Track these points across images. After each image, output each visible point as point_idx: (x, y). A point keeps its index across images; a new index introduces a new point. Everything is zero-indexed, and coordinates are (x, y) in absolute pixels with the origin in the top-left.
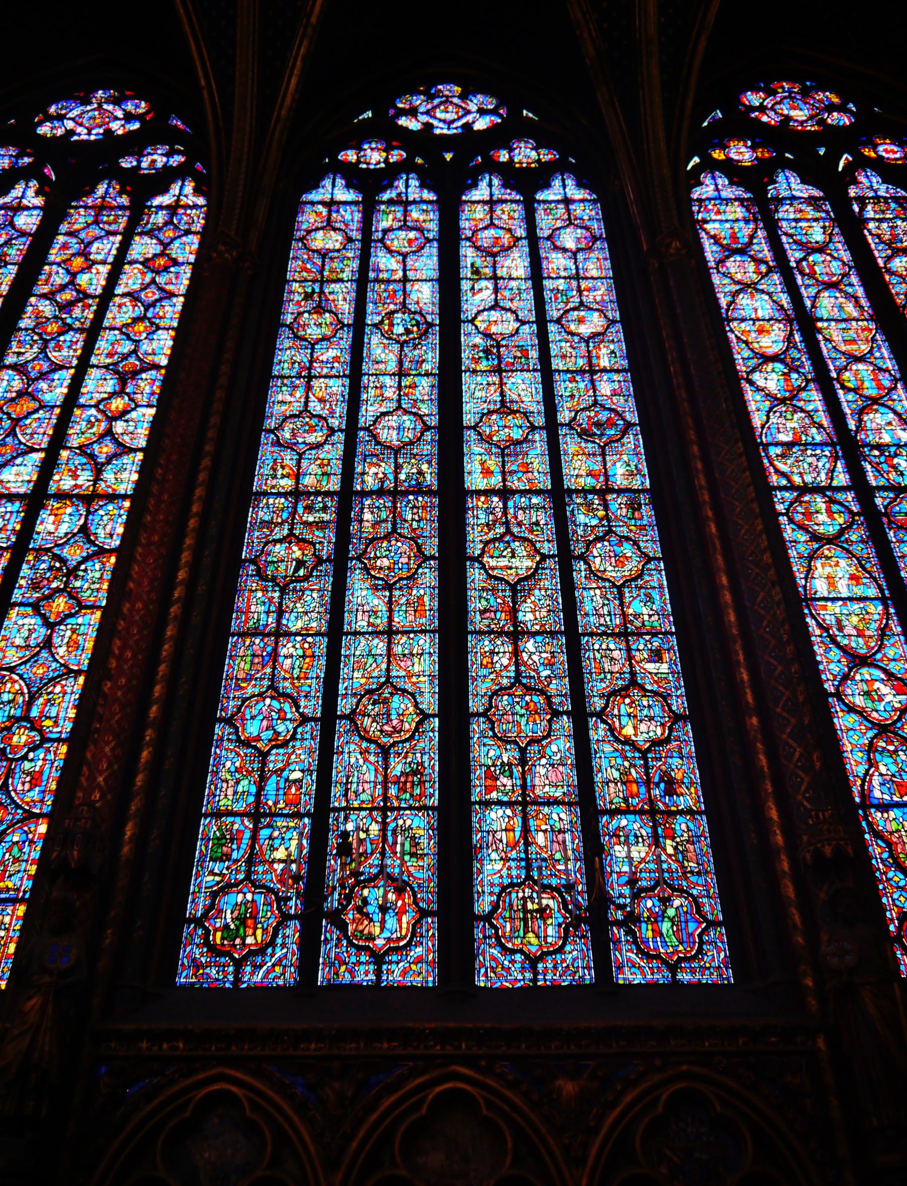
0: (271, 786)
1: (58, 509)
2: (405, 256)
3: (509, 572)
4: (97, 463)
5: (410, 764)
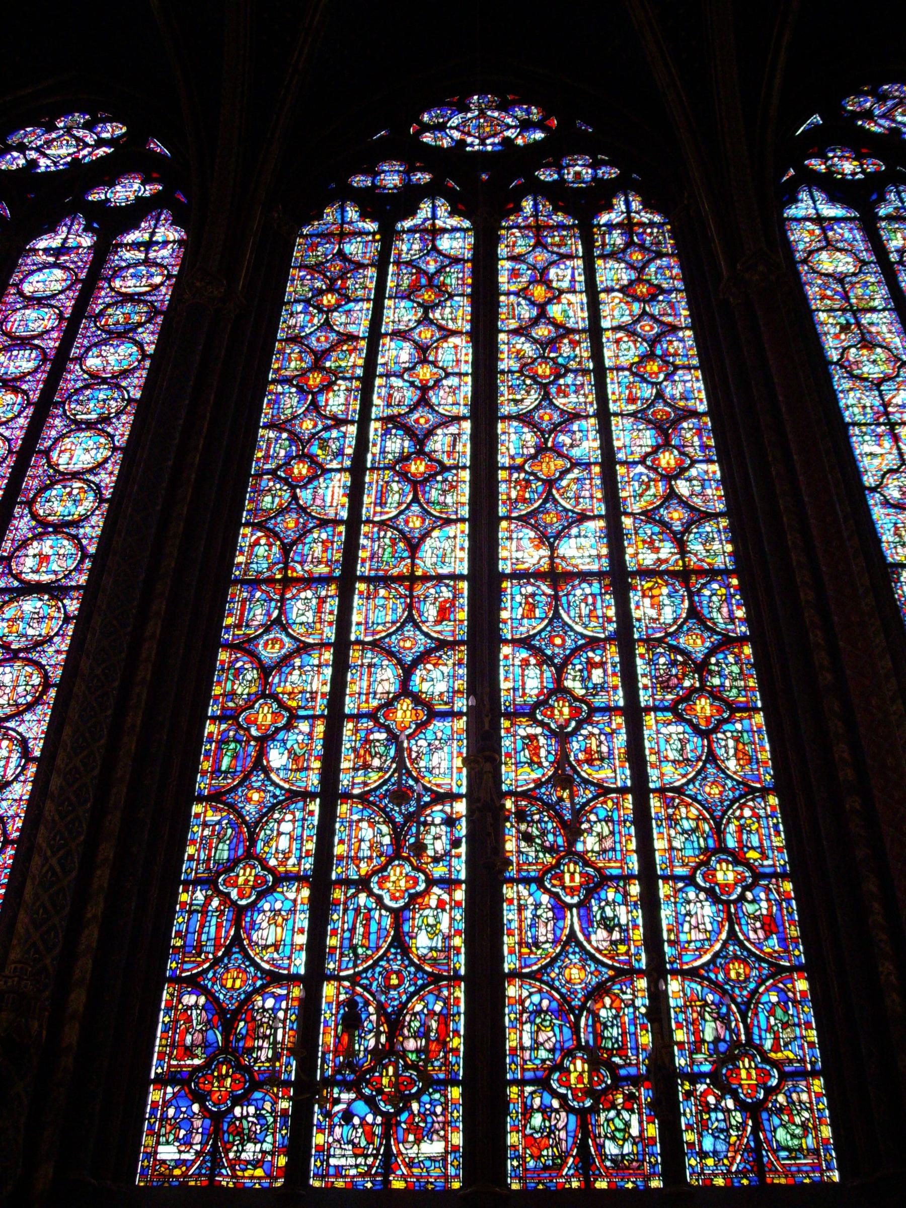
1: (650, 589)
4: (674, 533)
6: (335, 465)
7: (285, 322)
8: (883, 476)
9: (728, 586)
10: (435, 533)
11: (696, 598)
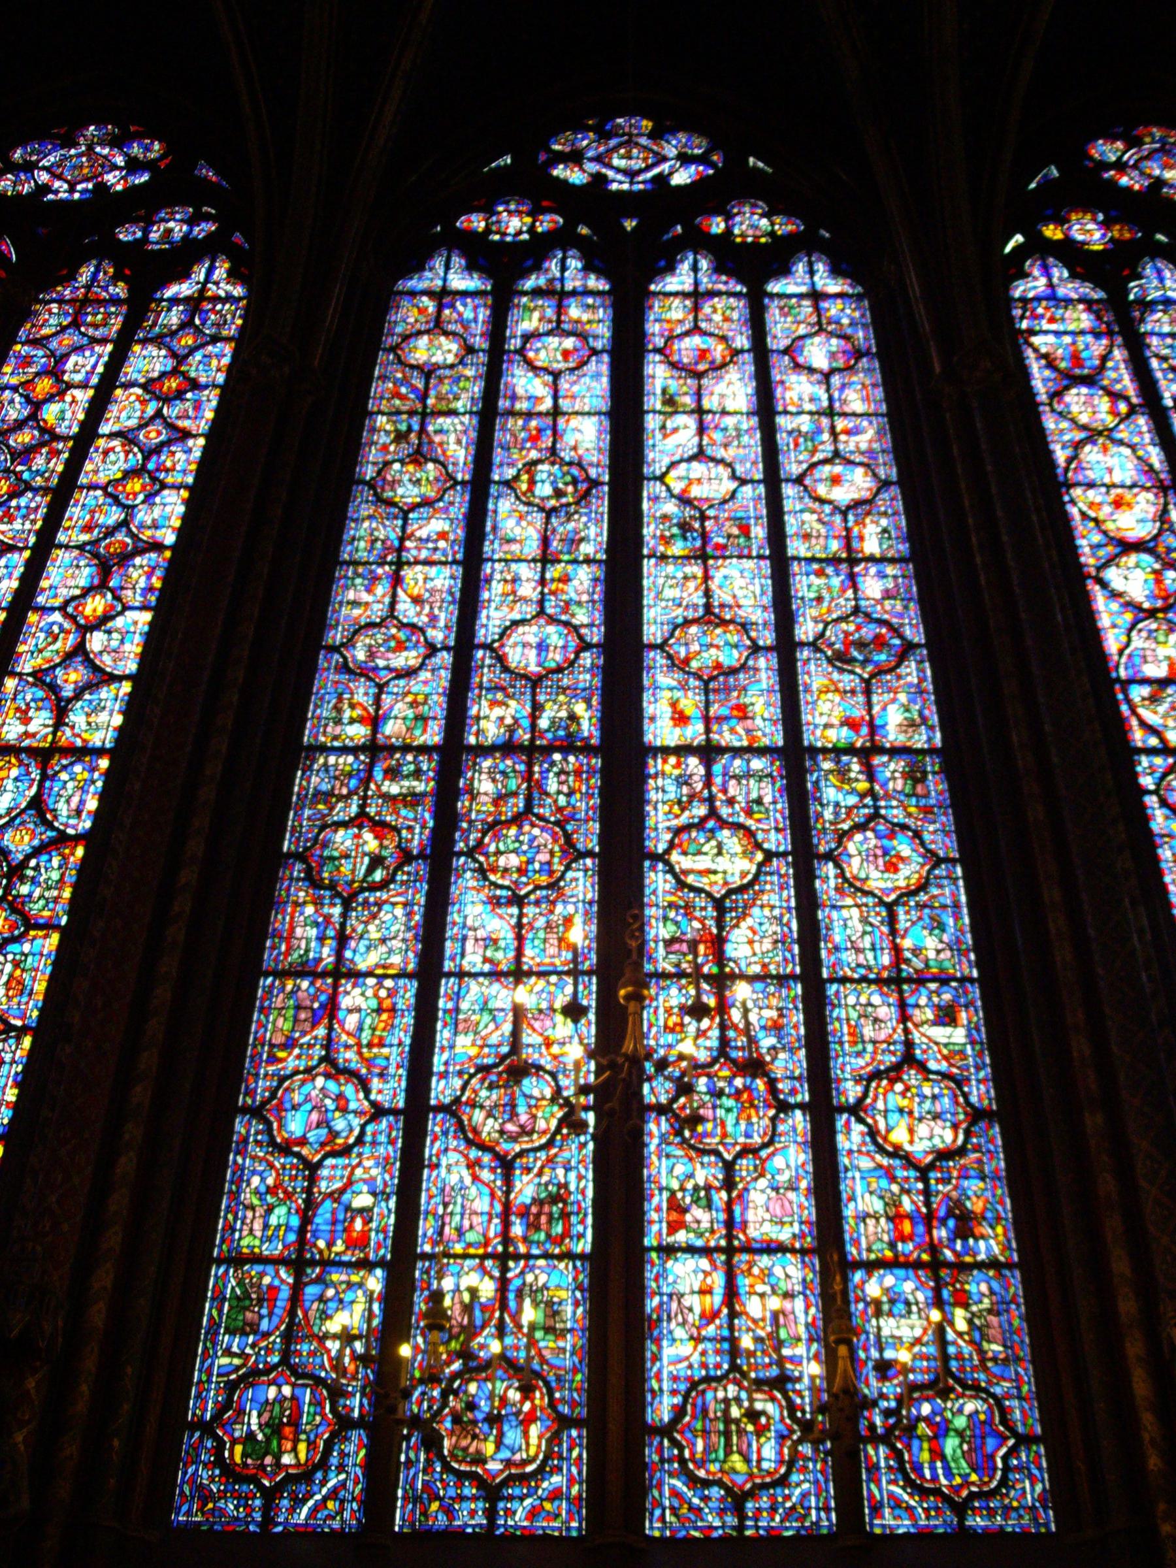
0: (322, 1217)
2: (556, 375)
3: (713, 877)
4: (59, 699)
5: (547, 1184)
8: (356, 632)
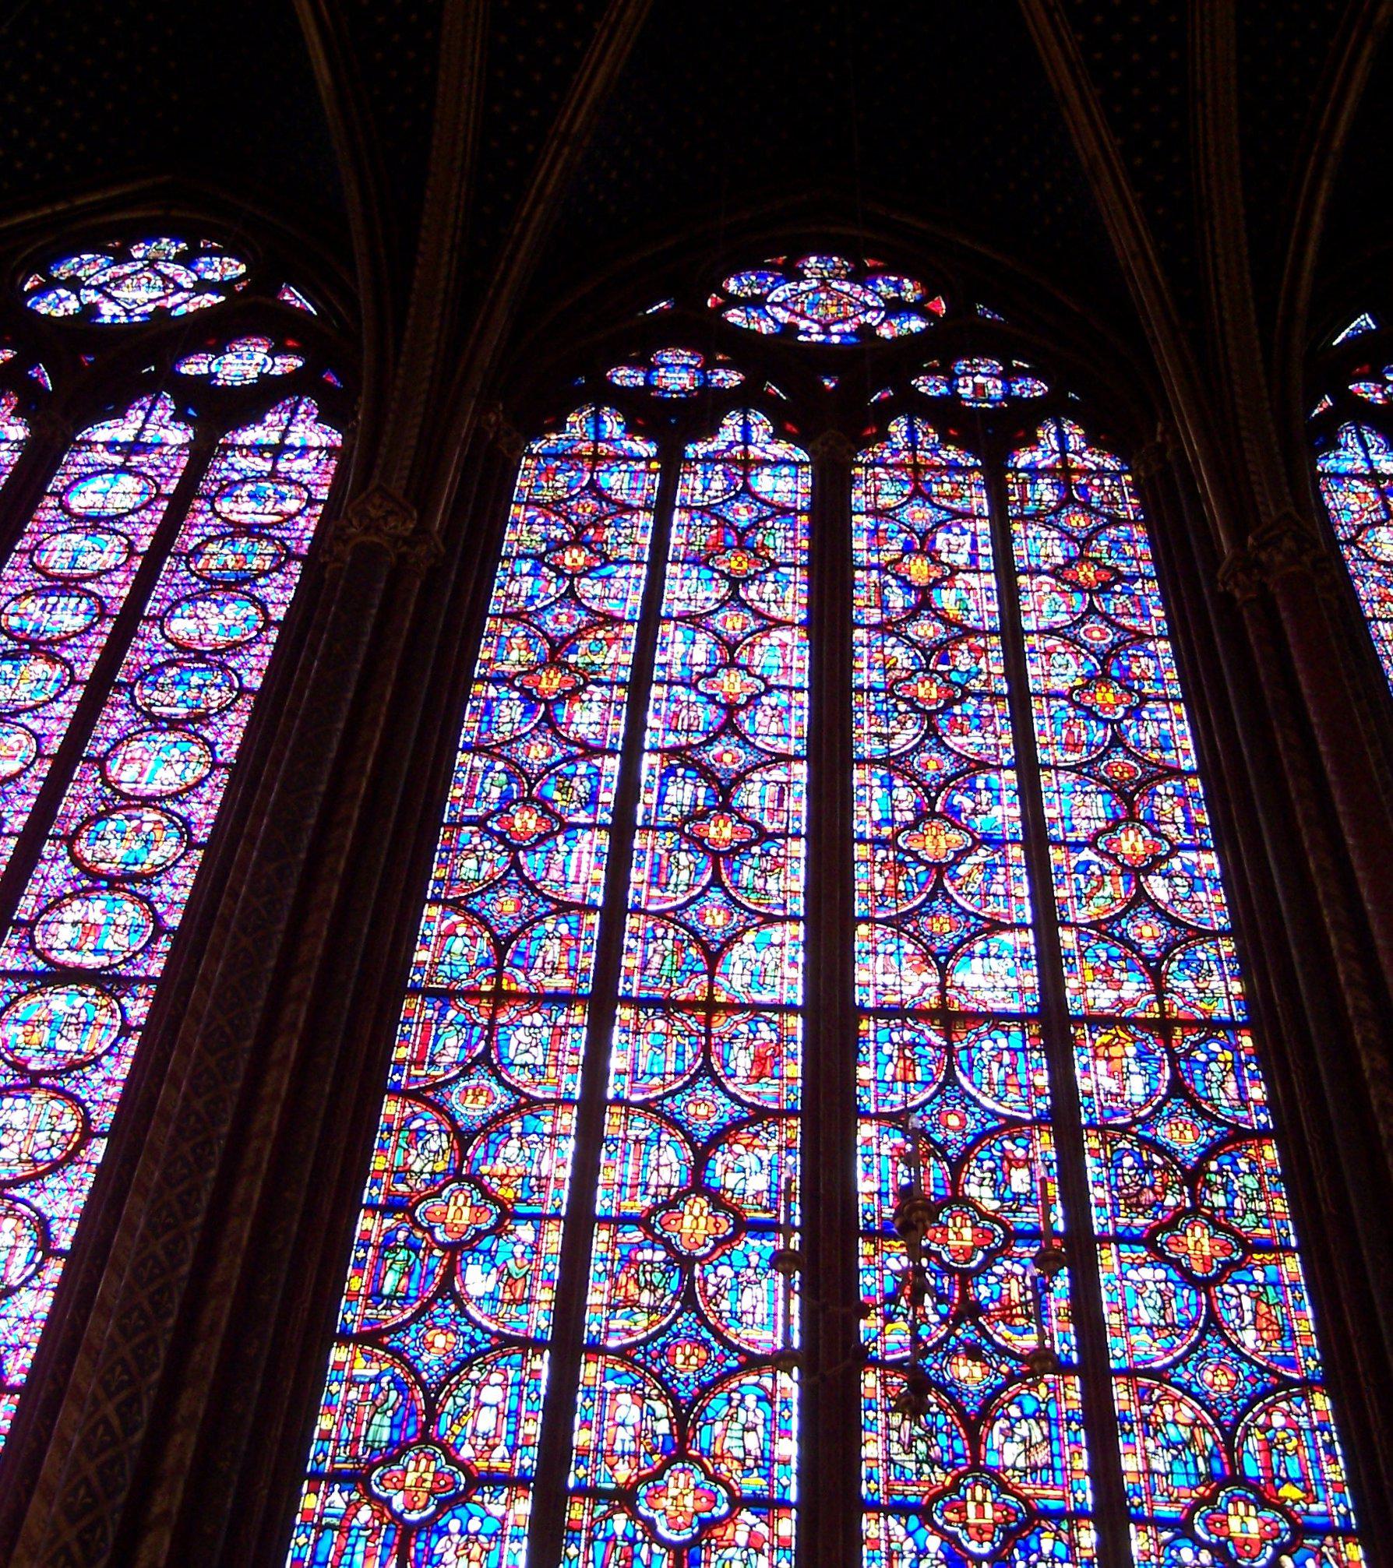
1: (1107, 1046)
4: (1146, 959)
6: (582, 817)
7: (501, 587)
9: (1235, 1049)
10: (750, 937)
11: (1183, 1065)
